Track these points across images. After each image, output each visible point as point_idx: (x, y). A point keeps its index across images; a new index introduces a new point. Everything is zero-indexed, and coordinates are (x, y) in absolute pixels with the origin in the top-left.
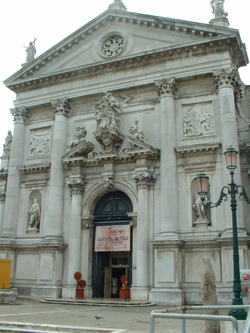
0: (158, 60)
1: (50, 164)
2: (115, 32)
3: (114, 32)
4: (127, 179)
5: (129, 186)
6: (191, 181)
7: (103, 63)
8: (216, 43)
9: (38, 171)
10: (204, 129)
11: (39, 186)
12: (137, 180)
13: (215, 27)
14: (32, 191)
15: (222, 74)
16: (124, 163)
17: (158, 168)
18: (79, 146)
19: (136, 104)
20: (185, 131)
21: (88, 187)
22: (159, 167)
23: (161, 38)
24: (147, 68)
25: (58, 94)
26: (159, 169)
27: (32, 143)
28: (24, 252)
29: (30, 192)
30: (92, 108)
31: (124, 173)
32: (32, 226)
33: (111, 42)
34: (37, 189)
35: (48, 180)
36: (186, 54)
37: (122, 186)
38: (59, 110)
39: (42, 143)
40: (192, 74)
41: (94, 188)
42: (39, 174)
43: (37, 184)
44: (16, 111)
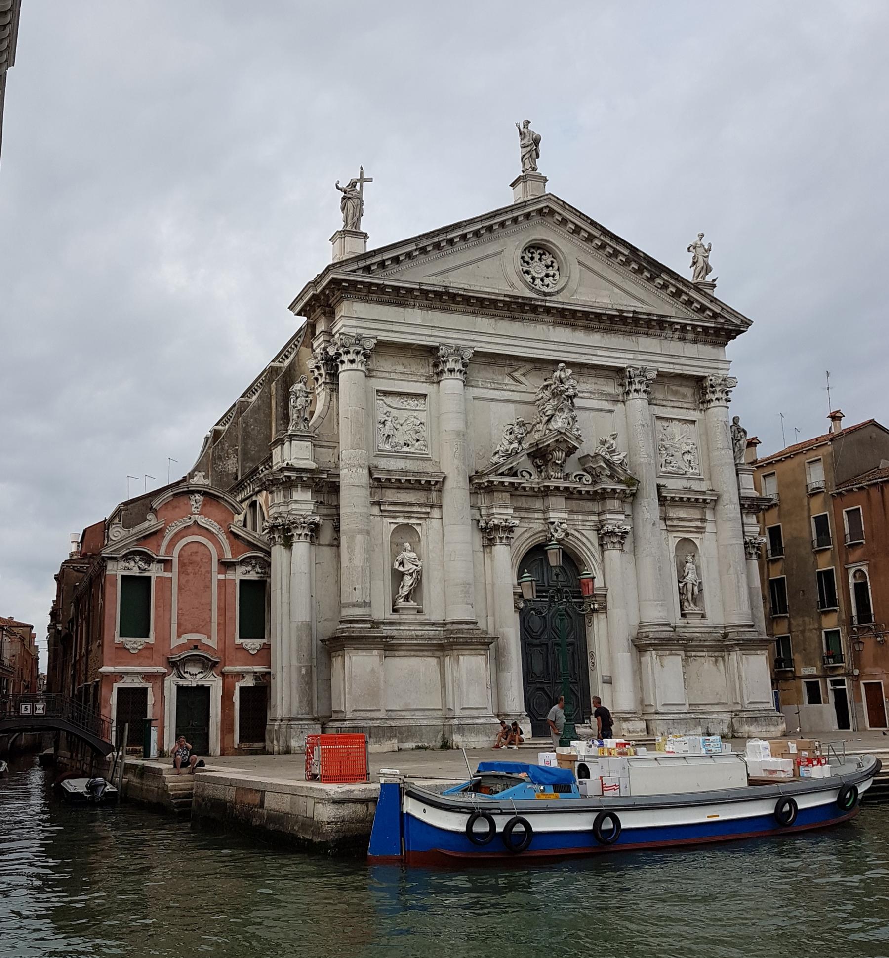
0: (628, 329)
1: (444, 478)
2: (548, 242)
3: (545, 241)
4: (580, 528)
5: (584, 540)
7: (547, 304)
8: (717, 331)
10: (688, 465)
11: (413, 517)
12: (612, 533)
13: (722, 305)
15: (720, 384)
18: (519, 456)
19: (586, 395)
20: (664, 462)
23: (626, 287)
24: (609, 335)
25: (450, 335)
28: (397, 653)
29: (393, 527)
30: (503, 380)
31: (575, 517)
32: (407, 598)
33: (530, 255)
34: (406, 521)
36: (670, 334)
37: (574, 539)
38: (456, 369)
39: (403, 427)
40: (678, 370)
41: (527, 535)
42: (412, 491)
44: (353, 341)
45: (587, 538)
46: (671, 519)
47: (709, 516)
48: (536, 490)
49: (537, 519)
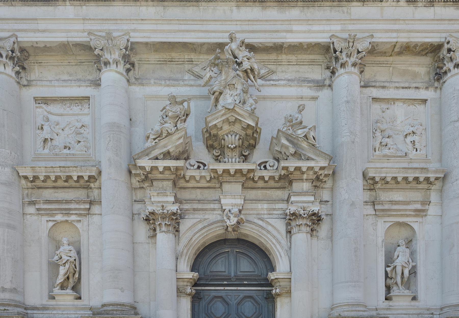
1: (100, 173)
4: (266, 216)
5: (270, 228)
6: (385, 230)
9: (66, 184)
14: (54, 223)
16: (259, 188)
17: (327, 203)
21: (185, 225)
22: (328, 202)
26: (326, 204)
27: (44, 127)
29: (51, 224)
31: (259, 206)
34: (66, 218)
35: (93, 204)
41: (200, 226)
43: (66, 209)
45: (273, 226)
46: (382, 203)
47: (434, 197)
48: (208, 179)
49: (214, 209)
